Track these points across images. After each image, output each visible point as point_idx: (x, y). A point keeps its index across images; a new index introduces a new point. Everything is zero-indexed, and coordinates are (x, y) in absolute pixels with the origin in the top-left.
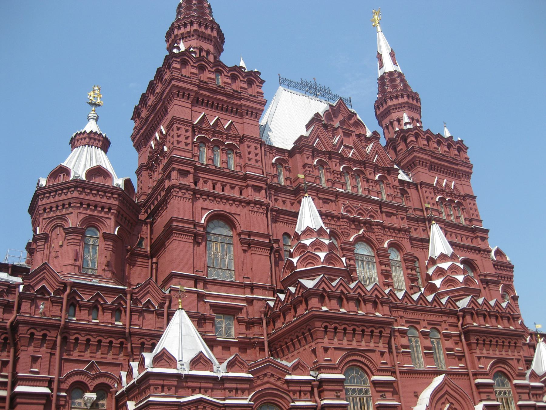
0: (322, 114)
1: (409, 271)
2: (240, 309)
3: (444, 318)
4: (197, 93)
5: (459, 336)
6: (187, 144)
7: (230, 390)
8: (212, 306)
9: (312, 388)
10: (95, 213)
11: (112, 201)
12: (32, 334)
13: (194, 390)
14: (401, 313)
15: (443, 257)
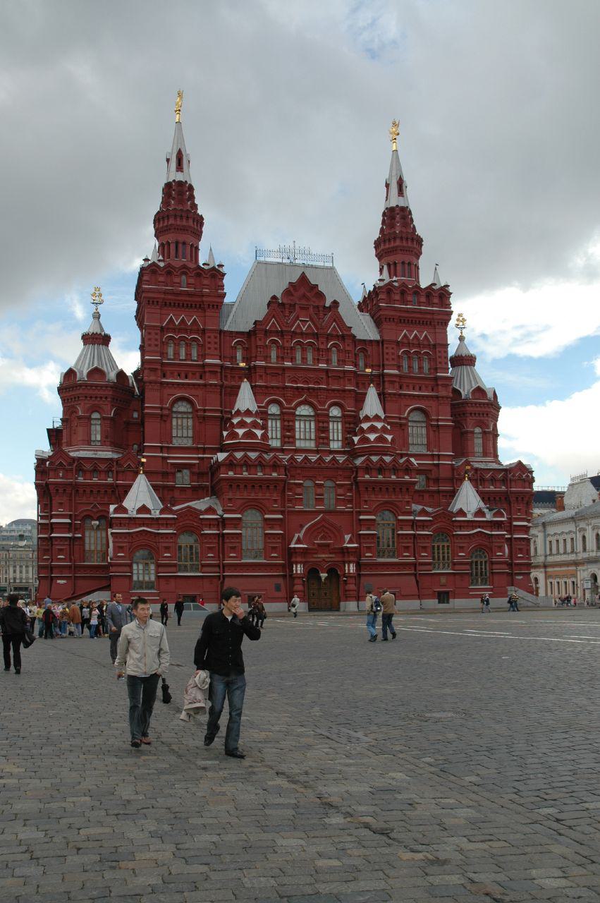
0: (279, 296)
1: (347, 425)
2: (194, 464)
3: (341, 473)
4: (164, 299)
5: (351, 485)
6: (156, 345)
7: (162, 524)
8: (172, 464)
9: (218, 522)
10: (96, 402)
11: (106, 393)
12: (57, 490)
13: (140, 526)
14: (299, 471)
15: (367, 419)
